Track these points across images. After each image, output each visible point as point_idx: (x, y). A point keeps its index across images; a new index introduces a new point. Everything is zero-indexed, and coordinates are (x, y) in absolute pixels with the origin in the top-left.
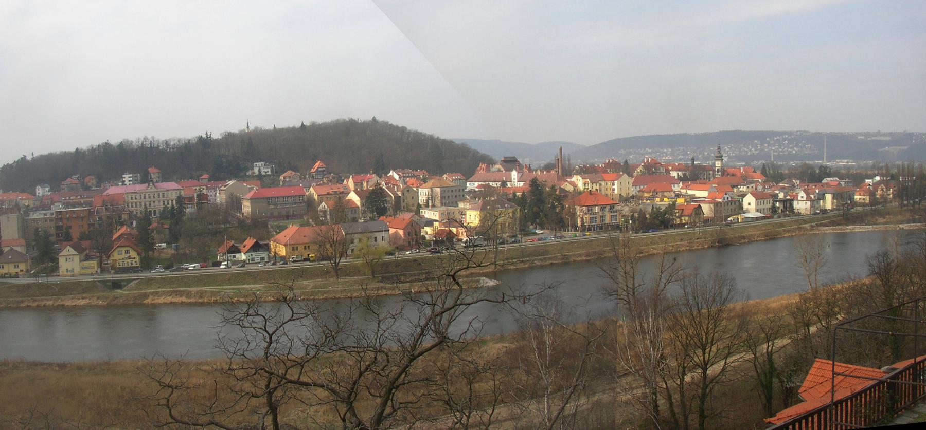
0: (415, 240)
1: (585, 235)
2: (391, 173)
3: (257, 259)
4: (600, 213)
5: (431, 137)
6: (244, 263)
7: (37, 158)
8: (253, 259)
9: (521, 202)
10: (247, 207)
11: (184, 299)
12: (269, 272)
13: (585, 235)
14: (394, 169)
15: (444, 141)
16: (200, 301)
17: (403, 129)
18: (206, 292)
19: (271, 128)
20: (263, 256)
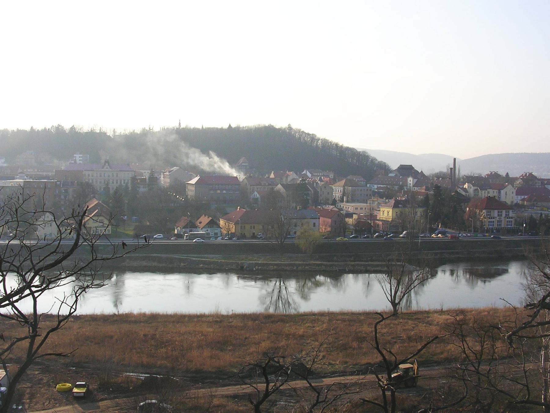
0: (339, 226)
1: (485, 236)
2: (304, 172)
3: (212, 234)
4: (497, 219)
5: (337, 145)
6: (201, 236)
7: (120, 136)
8: (208, 234)
9: (425, 203)
10: (191, 190)
11: (155, 264)
12: (225, 245)
13: (485, 236)
14: (308, 169)
15: (348, 149)
16: (170, 266)
17: (313, 138)
18: (176, 258)
19: (226, 126)
20: (216, 231)
